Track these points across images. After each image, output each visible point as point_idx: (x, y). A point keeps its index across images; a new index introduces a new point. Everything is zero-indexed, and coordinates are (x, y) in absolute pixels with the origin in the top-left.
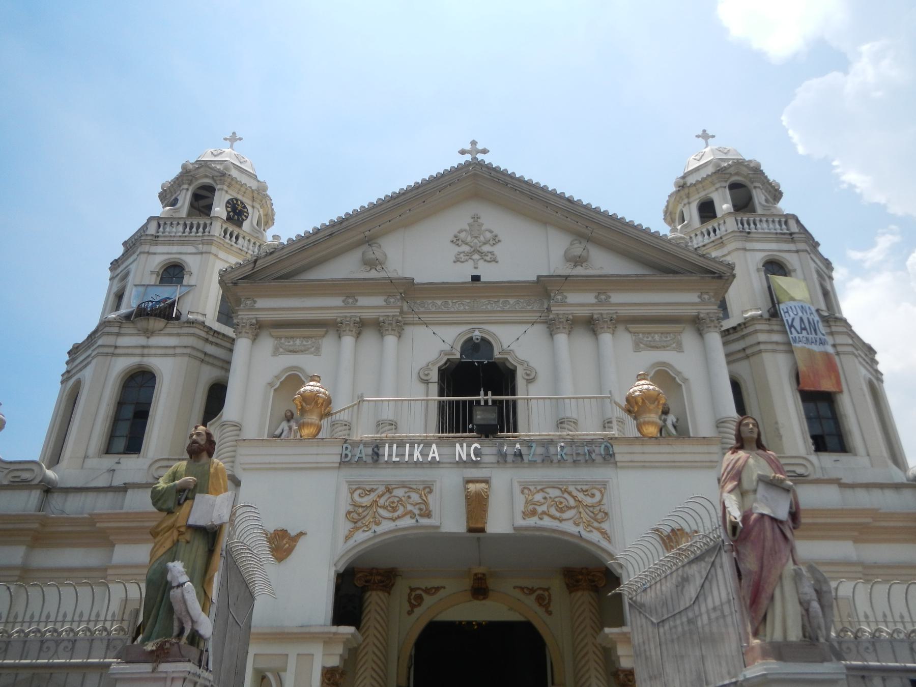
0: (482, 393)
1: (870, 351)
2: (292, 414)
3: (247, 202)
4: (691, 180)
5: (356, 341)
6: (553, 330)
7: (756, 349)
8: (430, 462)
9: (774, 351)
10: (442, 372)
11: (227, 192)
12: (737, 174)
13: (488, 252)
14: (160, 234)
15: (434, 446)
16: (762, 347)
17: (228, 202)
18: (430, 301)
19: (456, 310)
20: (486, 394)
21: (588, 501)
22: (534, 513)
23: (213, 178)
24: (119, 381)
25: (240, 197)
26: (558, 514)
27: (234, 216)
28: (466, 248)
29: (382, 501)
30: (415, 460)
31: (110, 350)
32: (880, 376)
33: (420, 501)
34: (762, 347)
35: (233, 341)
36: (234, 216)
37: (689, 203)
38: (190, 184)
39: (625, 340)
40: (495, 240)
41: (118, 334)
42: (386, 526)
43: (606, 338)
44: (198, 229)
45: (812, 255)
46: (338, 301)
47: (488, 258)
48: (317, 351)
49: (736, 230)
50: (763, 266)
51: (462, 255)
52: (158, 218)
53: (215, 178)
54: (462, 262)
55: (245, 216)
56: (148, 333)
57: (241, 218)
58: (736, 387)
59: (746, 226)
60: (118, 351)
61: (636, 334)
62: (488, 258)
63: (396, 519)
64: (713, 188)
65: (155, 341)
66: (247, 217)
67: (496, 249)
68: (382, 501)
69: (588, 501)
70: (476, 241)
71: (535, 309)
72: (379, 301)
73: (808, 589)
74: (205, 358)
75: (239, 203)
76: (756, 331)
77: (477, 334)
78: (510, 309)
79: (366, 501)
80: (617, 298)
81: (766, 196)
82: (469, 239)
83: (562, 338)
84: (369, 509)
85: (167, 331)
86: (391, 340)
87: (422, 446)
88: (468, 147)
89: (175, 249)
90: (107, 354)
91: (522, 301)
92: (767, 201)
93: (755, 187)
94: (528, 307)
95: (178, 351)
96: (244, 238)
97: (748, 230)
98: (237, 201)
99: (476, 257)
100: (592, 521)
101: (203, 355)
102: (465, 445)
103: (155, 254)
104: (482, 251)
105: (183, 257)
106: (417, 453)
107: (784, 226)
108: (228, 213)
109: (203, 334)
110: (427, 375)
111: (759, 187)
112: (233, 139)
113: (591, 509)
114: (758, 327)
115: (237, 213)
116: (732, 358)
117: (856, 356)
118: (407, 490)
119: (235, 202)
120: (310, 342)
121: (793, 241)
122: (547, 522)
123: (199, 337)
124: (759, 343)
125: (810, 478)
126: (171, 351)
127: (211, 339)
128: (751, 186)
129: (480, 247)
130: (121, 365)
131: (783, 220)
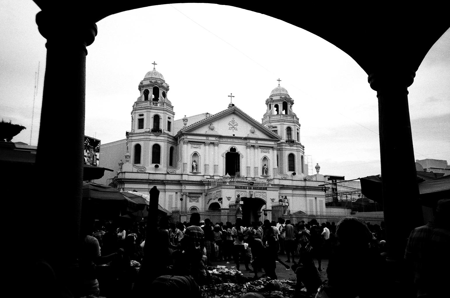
1: (304, 147)
7: (282, 149)
10: (226, 154)
12: (285, 100)
16: (283, 149)
21: (263, 195)
23: (159, 86)
25: (164, 91)
34: (283, 149)
39: (260, 150)
43: (256, 150)
46: (204, 138)
48: (200, 148)
50: (287, 129)
65: (159, 138)
72: (214, 139)
73: (288, 211)
74: (169, 142)
76: (283, 146)
80: (259, 142)
83: (248, 150)
85: (162, 135)
86: (216, 147)
89: (156, 111)
95: (164, 141)
105: (159, 114)
109: (168, 137)
114: (283, 145)
115: (164, 95)
117: (300, 152)
121: (294, 123)
122: (259, 197)
123: (168, 137)
124: (283, 148)
125: (286, 179)
126: (163, 141)
130: (152, 143)
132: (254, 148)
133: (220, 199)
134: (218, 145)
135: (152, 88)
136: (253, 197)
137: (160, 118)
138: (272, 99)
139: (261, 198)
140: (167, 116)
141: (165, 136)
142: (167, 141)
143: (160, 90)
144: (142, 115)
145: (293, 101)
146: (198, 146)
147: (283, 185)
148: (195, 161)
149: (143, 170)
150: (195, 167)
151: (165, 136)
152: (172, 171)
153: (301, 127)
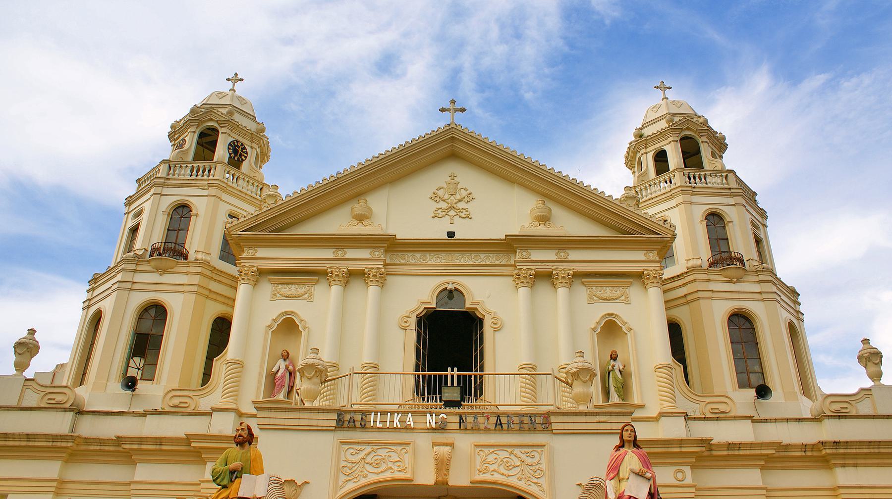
0: (449, 369)
2: (288, 354)
3: (247, 143)
4: (647, 132)
5: (344, 289)
6: (518, 284)
8: (406, 428)
9: (711, 298)
11: (229, 135)
12: (688, 129)
13: (462, 209)
14: (170, 176)
15: (410, 414)
16: (700, 294)
17: (230, 144)
18: (410, 254)
19: (433, 263)
20: (452, 370)
21: (529, 461)
22: (486, 471)
24: (135, 315)
25: (240, 139)
26: (506, 472)
27: (234, 157)
28: (444, 205)
29: (369, 459)
30: (395, 426)
31: (129, 285)
32: (800, 316)
33: (399, 459)
34: (700, 294)
35: (235, 279)
36: (234, 157)
37: (646, 153)
38: (197, 127)
39: (582, 292)
40: (470, 198)
43: (562, 291)
44: (204, 172)
45: (748, 207)
46: (328, 253)
48: (310, 299)
49: (684, 184)
51: (440, 211)
52: (169, 161)
53: (219, 122)
54: (439, 218)
55: (245, 156)
56: (163, 271)
57: (242, 159)
58: (675, 331)
59: (692, 180)
60: (136, 286)
61: (590, 288)
63: (379, 473)
64: (667, 142)
65: (168, 278)
66: (246, 157)
68: (369, 459)
69: (529, 461)
70: (452, 198)
71: (502, 263)
72: (364, 254)
74: (211, 295)
75: (240, 144)
77: (450, 287)
78: (481, 263)
80: (574, 255)
81: (712, 149)
82: (446, 197)
83: (523, 291)
84: (358, 465)
86: (373, 290)
87: (400, 415)
88: (447, 105)
90: (125, 289)
91: (491, 255)
92: (713, 155)
93: (702, 142)
94: (497, 262)
96: (243, 179)
97: (693, 185)
98: (238, 143)
99: (452, 213)
100: (531, 477)
101: (208, 292)
102: (434, 415)
103: (166, 195)
104: (458, 208)
106: (396, 420)
107: (724, 181)
108: (230, 154)
109: (208, 273)
110: (406, 322)
111: (706, 142)
112: (236, 79)
113: (531, 468)
115: (237, 155)
116: (670, 304)
118: (389, 450)
119: (236, 144)
120: (303, 290)
121: (731, 195)
122: (497, 477)
125: (728, 415)
127: (214, 276)
128: (700, 140)
129: (455, 204)
130: (139, 299)
131: (724, 175)
132: (554, 285)
134: (381, 280)
135: (193, 129)
136: (459, 479)
137: (194, 211)
138: (641, 136)
139: (514, 481)
140: (224, 210)
141: (192, 269)
142: (195, 289)
143: (220, 133)
144: (139, 214)
145: (724, 138)
146: (302, 290)
147: (705, 443)
148: (286, 356)
150: (283, 376)
151: (192, 269)
153: (768, 222)
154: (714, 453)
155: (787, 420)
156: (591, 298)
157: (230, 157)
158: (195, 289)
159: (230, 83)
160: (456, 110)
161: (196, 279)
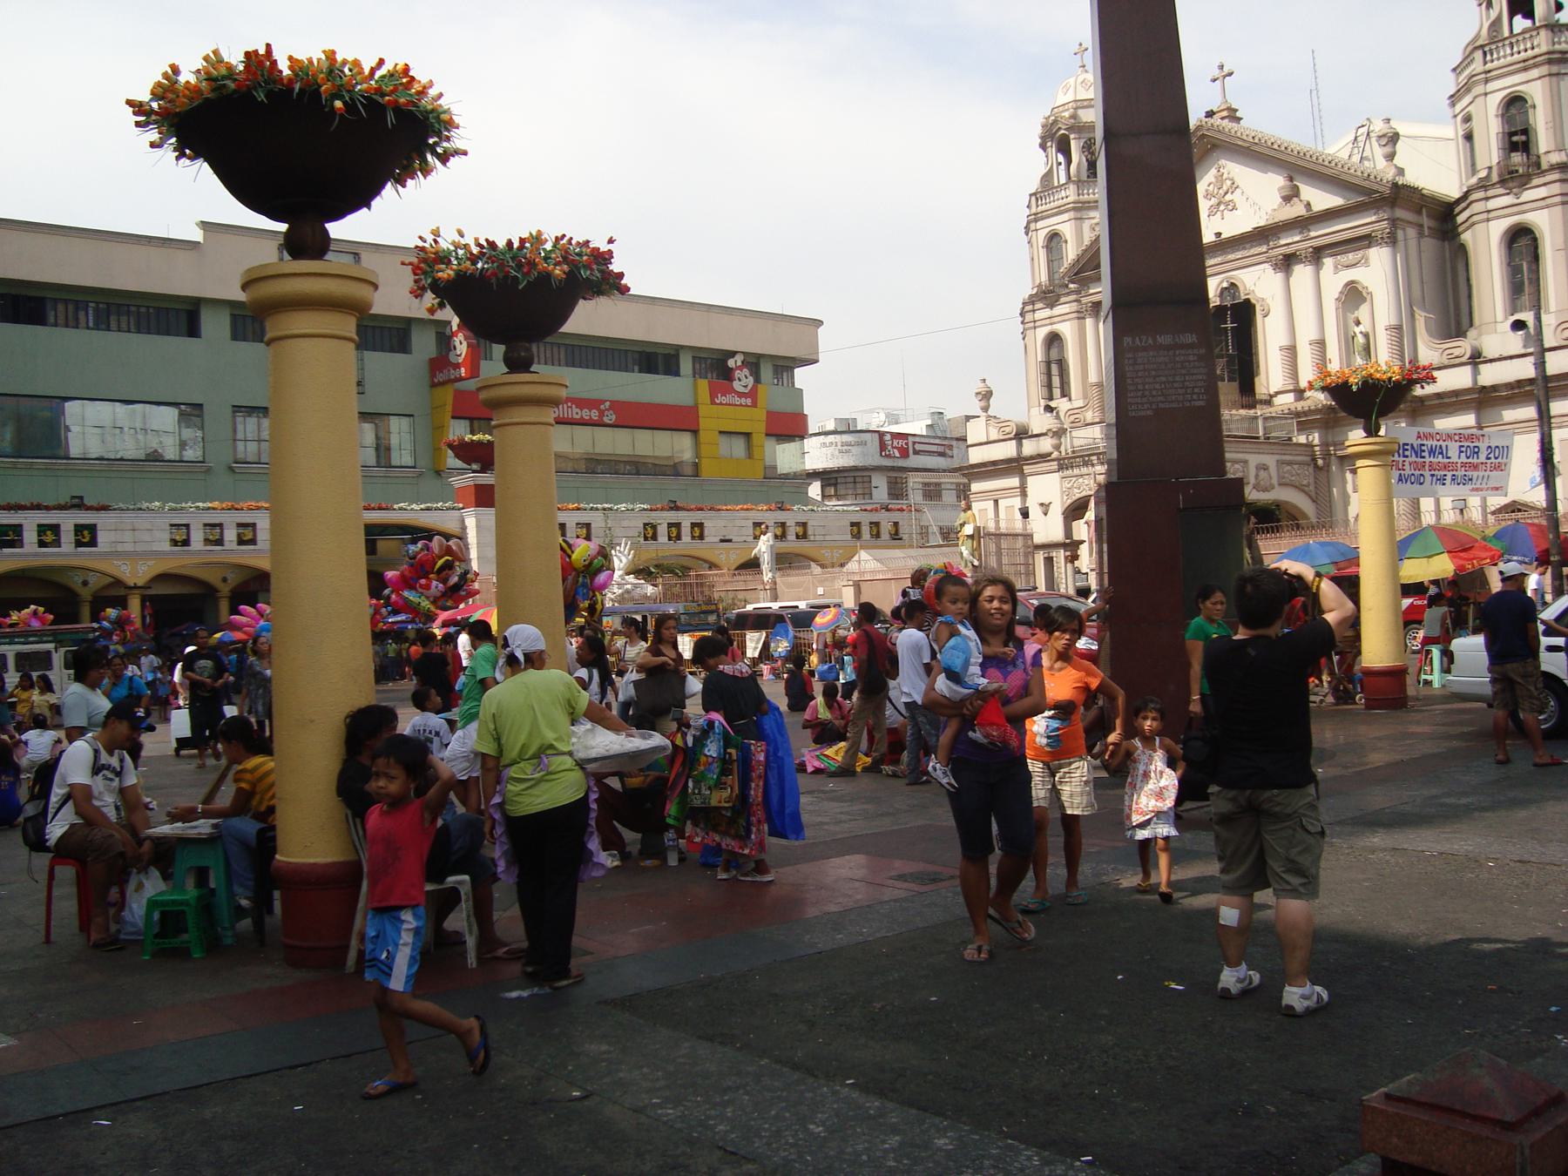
9: (1488, 220)
16: (1475, 218)
17: (1083, 147)
40: (1234, 187)
41: (1034, 311)
42: (1078, 496)
47: (1230, 207)
52: (1035, 194)
56: (1051, 306)
62: (1230, 207)
67: (1235, 197)
70: (1221, 191)
76: (1472, 202)
77: (1225, 285)
79: (1069, 486)
88: (1217, 73)
99: (1222, 207)
130: (1042, 333)
133: (1025, 514)
142: (1075, 315)
149: (1008, 430)
152: (1072, 418)
154: (1426, 403)
155: (1511, 357)
156: (1336, 267)
157: (1087, 160)
158: (1075, 315)
159: (1079, 56)
160: (1224, 77)
161: (1074, 306)
